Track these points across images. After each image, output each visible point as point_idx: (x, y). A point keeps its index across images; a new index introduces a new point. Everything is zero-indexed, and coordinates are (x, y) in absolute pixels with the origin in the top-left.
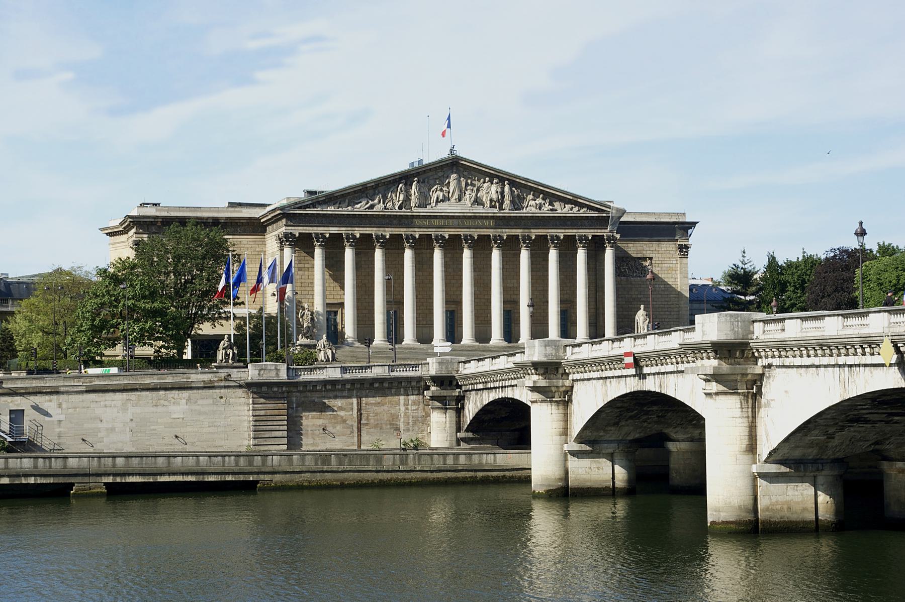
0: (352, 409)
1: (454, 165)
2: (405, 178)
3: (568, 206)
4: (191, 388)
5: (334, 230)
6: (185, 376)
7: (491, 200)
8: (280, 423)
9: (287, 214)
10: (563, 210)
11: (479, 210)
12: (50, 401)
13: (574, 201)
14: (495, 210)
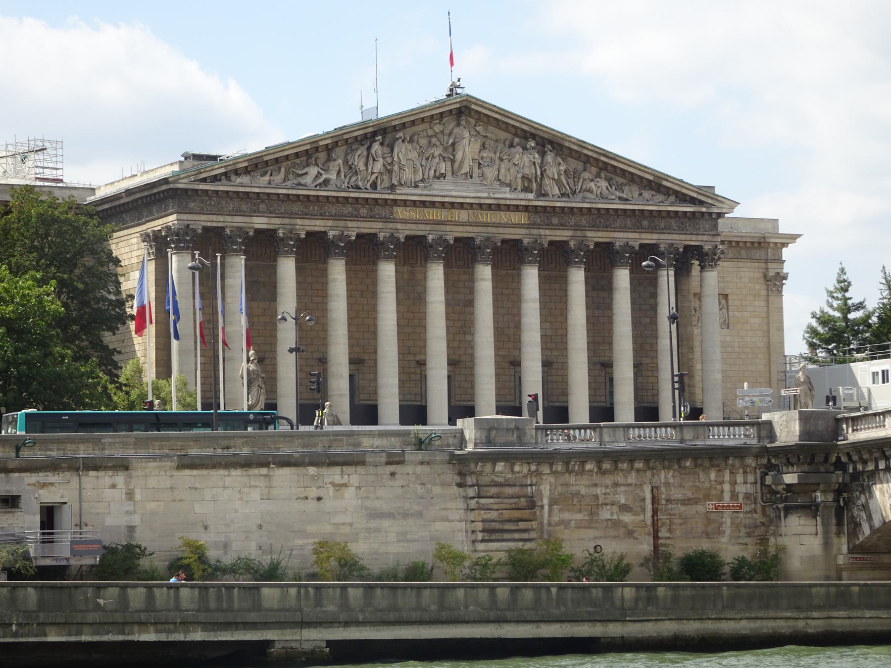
0: (644, 510)
1: (462, 111)
3: (647, 194)
4: (362, 463)
5: (260, 222)
6: (351, 440)
7: (523, 177)
8: (525, 536)
11: (506, 195)
12: (114, 486)
13: (655, 183)
14: (531, 196)
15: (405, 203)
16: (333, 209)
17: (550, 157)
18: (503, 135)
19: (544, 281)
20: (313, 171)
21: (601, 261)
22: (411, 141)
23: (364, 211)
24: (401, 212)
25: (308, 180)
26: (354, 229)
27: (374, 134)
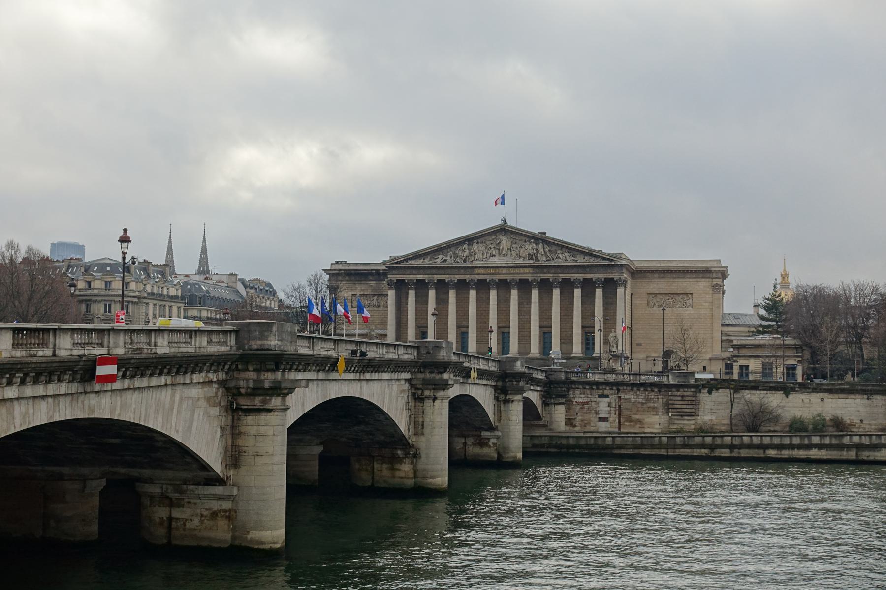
1: (504, 229)
2: (469, 240)
5: (420, 277)
9: (396, 265)
10: (582, 260)
11: (521, 261)
13: (590, 253)
15: (476, 267)
16: (449, 271)
17: (541, 246)
18: (524, 238)
19: (478, 300)
20: (440, 257)
21: (567, 286)
22: (482, 243)
23: (462, 271)
24: (477, 271)
25: (438, 261)
26: (456, 278)
27: (464, 241)
